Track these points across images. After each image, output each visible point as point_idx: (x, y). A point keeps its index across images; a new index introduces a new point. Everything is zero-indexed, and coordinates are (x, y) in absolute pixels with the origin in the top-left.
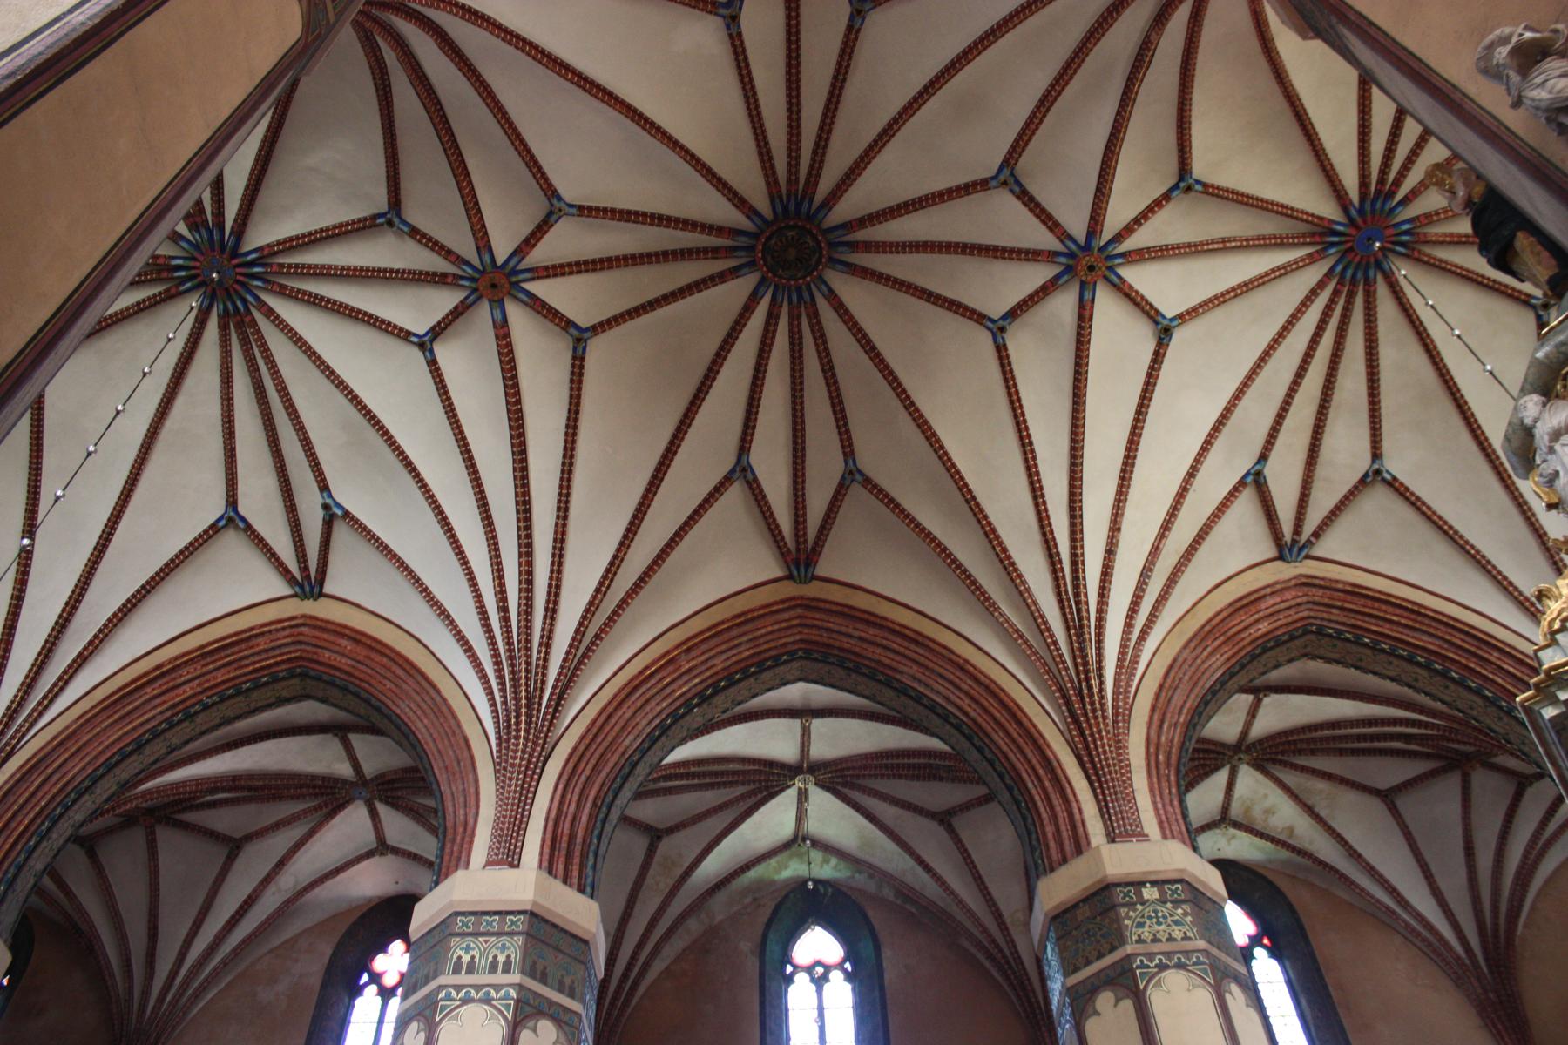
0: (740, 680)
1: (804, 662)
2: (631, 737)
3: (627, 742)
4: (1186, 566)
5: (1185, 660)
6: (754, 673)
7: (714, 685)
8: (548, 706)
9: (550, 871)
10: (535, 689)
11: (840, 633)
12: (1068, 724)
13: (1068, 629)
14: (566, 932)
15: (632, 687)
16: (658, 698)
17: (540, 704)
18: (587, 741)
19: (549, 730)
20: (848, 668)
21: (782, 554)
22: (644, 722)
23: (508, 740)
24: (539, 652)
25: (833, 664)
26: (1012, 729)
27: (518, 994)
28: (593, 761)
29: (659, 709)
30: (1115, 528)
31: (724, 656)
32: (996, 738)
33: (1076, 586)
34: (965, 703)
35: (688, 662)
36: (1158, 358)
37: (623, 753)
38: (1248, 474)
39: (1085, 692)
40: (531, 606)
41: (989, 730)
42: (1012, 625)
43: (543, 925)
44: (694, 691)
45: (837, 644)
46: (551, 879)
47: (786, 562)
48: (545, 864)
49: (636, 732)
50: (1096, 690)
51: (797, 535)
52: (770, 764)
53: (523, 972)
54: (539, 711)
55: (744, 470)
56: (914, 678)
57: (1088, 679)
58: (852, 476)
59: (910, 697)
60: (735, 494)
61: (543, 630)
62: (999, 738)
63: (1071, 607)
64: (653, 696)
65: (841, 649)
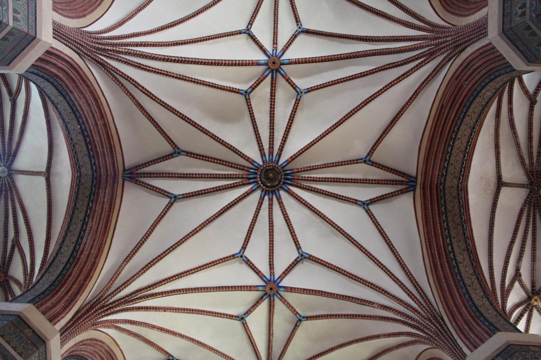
0: (88, 147)
1: (91, 176)
2: (77, 96)
3: (76, 94)
4: (140, 340)
5: (102, 347)
6: (89, 154)
7: (88, 136)
8: (100, 58)
9: (48, 52)
10: (109, 54)
11: (105, 193)
12: (89, 302)
13: (127, 296)
14: (18, 55)
15: (96, 99)
16: (89, 110)
17: (102, 55)
18: (83, 75)
19: (91, 57)
20: (90, 197)
21: (136, 167)
22: (81, 103)
23: (90, 37)
24: (123, 58)
25: (92, 190)
26: (82, 277)
27: (5, 24)
28: (74, 77)
29: (85, 110)
30: (165, 309)
31: (99, 141)
32: (76, 269)
33: (141, 298)
34: (86, 253)
35: (100, 125)
36: (231, 317)
37: (71, 92)
38: (172, 356)
39: (105, 309)
40: (143, 57)
41: (78, 265)
42: (122, 270)
43: (27, 43)
44: (87, 126)
45: (100, 191)
46: (45, 51)
47: (132, 168)
48: (51, 50)
49: (78, 99)
50: (107, 313)
51: (144, 174)
52: (15, 155)
53: (13, 28)
54: (100, 54)
55: (179, 153)
56: (91, 228)
57: (110, 308)
58: (174, 199)
59: (82, 227)
60: (168, 149)
61: (132, 61)
62: (76, 270)
63: (136, 296)
64: (90, 108)
65: (98, 194)
